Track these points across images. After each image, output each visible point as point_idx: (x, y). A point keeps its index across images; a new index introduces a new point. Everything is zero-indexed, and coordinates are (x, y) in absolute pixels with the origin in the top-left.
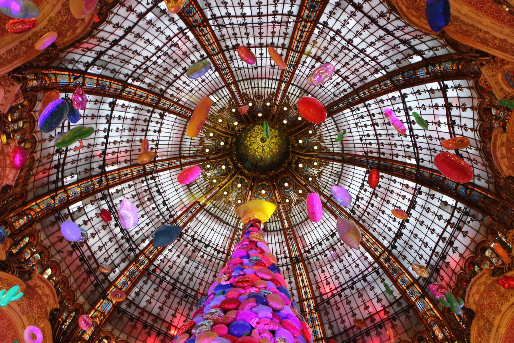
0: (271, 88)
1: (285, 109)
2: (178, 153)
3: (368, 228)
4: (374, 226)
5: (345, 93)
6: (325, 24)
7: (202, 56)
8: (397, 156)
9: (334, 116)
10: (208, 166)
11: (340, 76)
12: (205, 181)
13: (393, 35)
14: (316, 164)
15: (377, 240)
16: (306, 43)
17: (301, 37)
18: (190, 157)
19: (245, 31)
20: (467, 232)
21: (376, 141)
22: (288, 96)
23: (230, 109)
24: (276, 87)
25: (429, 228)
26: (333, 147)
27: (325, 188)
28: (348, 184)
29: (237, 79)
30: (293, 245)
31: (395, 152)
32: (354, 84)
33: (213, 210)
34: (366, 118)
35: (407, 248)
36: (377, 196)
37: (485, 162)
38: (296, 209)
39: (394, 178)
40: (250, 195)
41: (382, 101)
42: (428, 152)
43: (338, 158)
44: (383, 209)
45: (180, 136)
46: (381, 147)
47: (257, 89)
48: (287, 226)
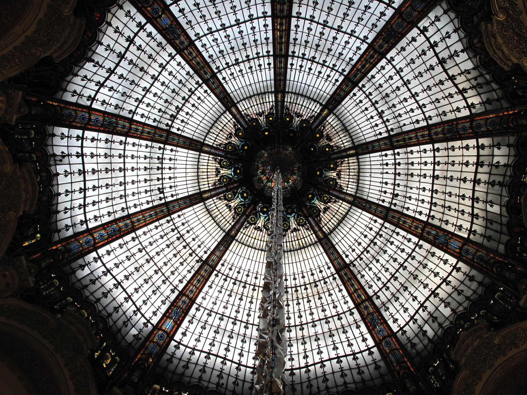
0: (269, 102)
9: (334, 112)
12: (230, 210)
14: (332, 166)
15: (414, 218)
16: (288, 43)
20: (498, 162)
25: (460, 179)
26: (343, 144)
27: (347, 187)
28: (368, 175)
30: (333, 254)
31: (402, 123)
32: (344, 70)
35: (446, 211)
37: (487, 77)
38: (325, 217)
39: (409, 149)
41: (373, 77)
42: (433, 106)
46: (387, 124)
47: (256, 106)
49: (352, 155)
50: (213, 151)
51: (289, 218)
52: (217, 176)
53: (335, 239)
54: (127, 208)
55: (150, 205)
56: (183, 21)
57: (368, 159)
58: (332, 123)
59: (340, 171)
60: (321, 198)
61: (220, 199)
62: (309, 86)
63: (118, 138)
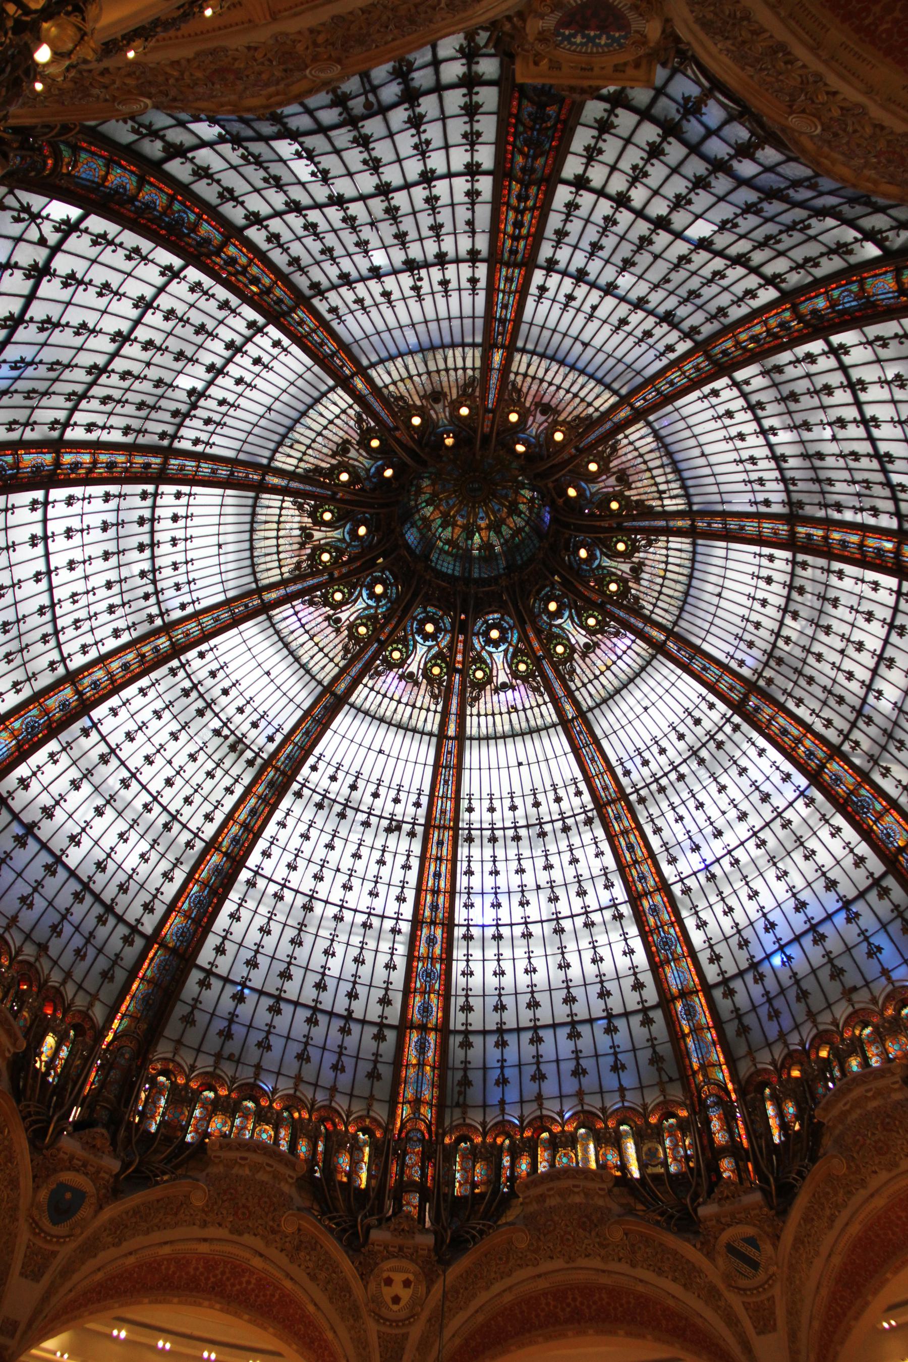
0: (464, 369)
1: (514, 417)
2: (250, 579)
3: (782, 699)
4: (798, 693)
5: (672, 356)
6: (581, 183)
7: (251, 325)
8: (839, 507)
9: (651, 418)
10: (338, 596)
11: (651, 313)
12: (338, 631)
13: (785, 199)
14: (621, 547)
16: (537, 238)
17: (518, 224)
18: (284, 583)
19: (354, 238)
21: (776, 474)
22: (514, 383)
23: (364, 443)
24: (478, 364)
29: (365, 362)
32: (694, 330)
34: (740, 417)
36: (795, 616)
39: (836, 566)
40: (460, 646)
41: (779, 369)
43: (680, 523)
44: (817, 648)
45: (246, 536)
48: (570, 711)
49: (679, 532)
50: (294, 485)
51: (490, 654)
53: (602, 724)
54: (63, 660)
55: (125, 638)
56: (206, 191)
57: (722, 553)
58: (638, 444)
60: (579, 616)
61: (311, 603)
62: (586, 345)
63: (24, 498)
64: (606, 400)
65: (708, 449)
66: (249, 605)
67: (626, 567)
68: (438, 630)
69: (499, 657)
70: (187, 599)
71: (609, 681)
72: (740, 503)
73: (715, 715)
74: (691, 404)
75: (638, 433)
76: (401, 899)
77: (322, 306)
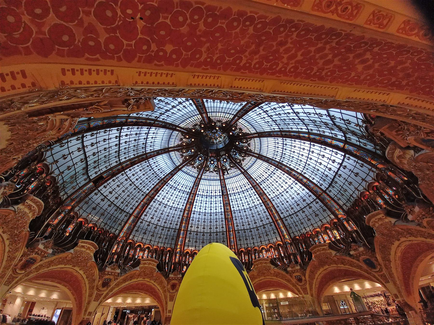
12: (195, 168)
18: (181, 164)
33: (206, 177)
38: (244, 163)
52: (182, 157)
59: (250, 144)
64: (231, 117)
65: (257, 121)
66: (177, 169)
67: (247, 144)
68: (214, 162)
69: (227, 164)
70: (164, 173)
71: (249, 164)
72: (267, 129)
73: (272, 168)
74: (251, 113)
75: (241, 120)
76: (221, 209)
77: (161, 120)
